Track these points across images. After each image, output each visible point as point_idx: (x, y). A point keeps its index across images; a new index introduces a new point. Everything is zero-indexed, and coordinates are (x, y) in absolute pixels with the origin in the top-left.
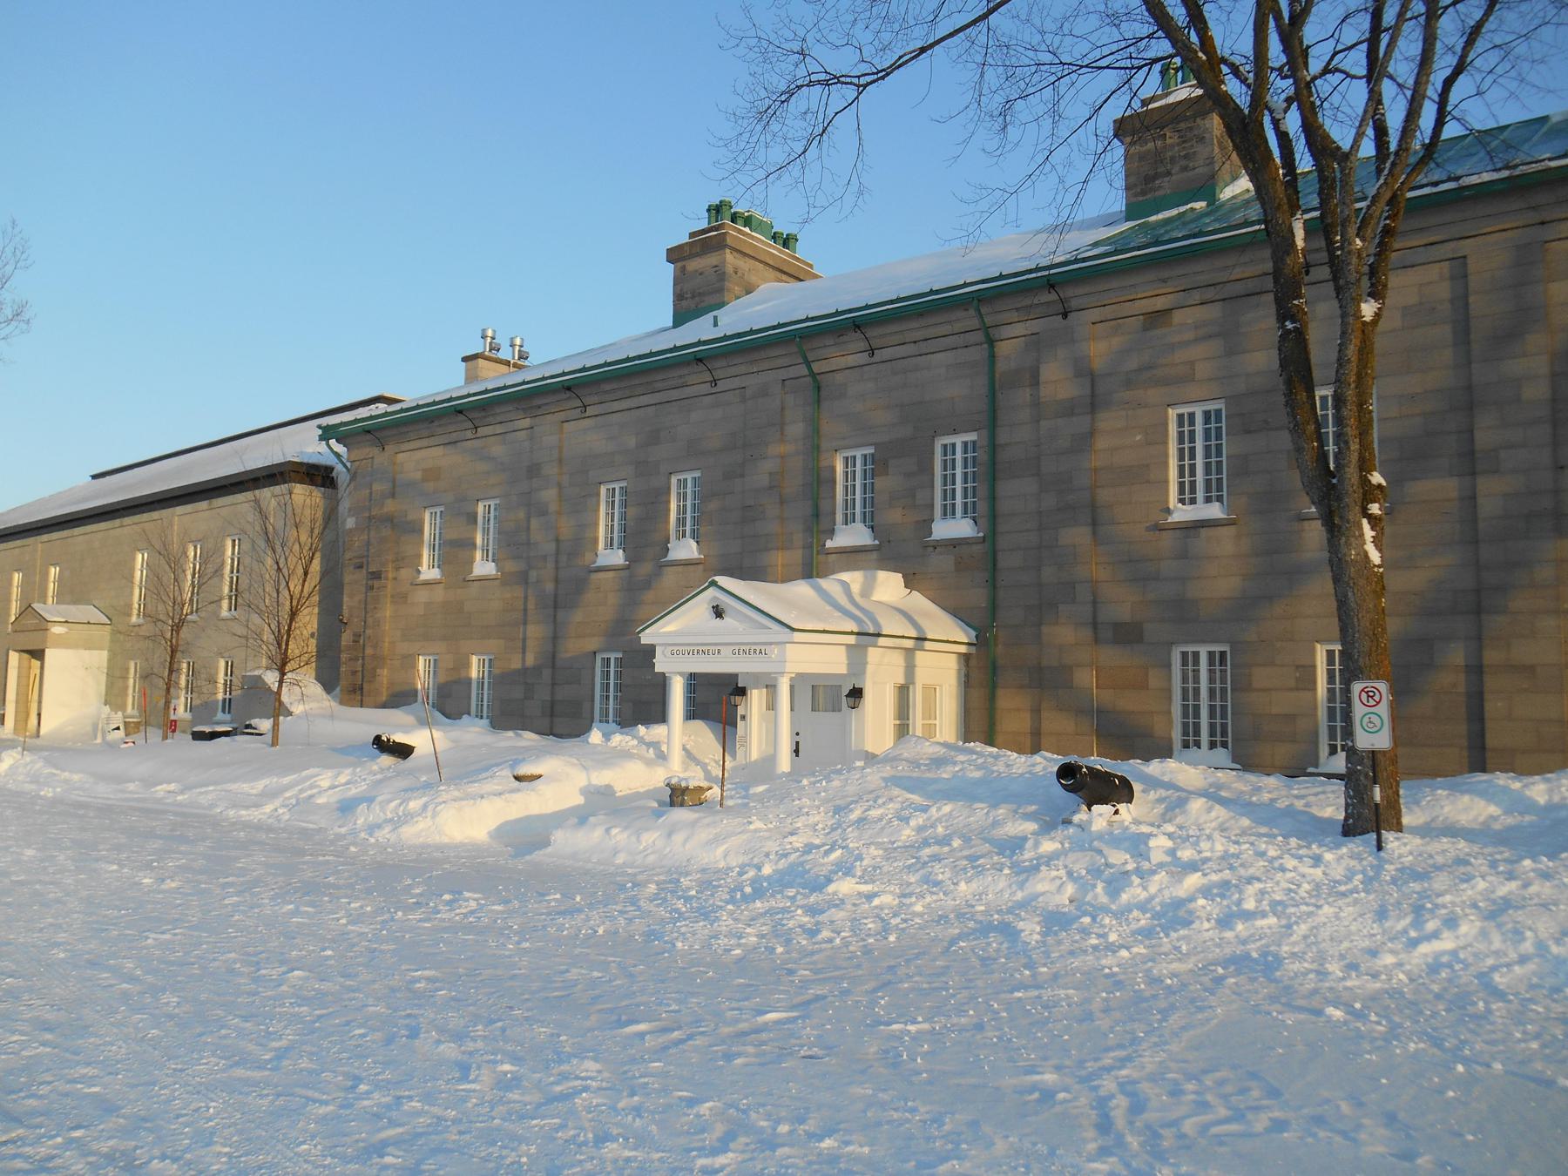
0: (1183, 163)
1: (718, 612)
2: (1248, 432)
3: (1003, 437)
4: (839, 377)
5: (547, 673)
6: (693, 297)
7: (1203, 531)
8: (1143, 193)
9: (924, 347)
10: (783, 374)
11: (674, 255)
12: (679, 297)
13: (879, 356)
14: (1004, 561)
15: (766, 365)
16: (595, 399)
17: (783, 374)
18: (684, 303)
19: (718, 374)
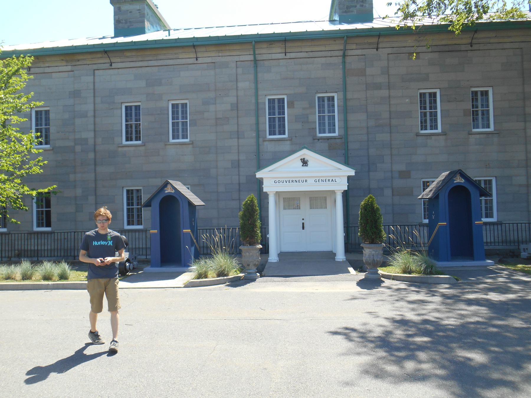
0: (362, 4)
1: (305, 162)
2: (449, 102)
4: (266, 63)
6: (126, 23)
7: (433, 137)
8: (346, 12)
9: (311, 54)
10: (237, 58)
12: (117, 22)
13: (289, 56)
14: (351, 146)
15: (228, 54)
16: (119, 60)
17: (237, 58)
18: (121, 25)
19: (199, 55)
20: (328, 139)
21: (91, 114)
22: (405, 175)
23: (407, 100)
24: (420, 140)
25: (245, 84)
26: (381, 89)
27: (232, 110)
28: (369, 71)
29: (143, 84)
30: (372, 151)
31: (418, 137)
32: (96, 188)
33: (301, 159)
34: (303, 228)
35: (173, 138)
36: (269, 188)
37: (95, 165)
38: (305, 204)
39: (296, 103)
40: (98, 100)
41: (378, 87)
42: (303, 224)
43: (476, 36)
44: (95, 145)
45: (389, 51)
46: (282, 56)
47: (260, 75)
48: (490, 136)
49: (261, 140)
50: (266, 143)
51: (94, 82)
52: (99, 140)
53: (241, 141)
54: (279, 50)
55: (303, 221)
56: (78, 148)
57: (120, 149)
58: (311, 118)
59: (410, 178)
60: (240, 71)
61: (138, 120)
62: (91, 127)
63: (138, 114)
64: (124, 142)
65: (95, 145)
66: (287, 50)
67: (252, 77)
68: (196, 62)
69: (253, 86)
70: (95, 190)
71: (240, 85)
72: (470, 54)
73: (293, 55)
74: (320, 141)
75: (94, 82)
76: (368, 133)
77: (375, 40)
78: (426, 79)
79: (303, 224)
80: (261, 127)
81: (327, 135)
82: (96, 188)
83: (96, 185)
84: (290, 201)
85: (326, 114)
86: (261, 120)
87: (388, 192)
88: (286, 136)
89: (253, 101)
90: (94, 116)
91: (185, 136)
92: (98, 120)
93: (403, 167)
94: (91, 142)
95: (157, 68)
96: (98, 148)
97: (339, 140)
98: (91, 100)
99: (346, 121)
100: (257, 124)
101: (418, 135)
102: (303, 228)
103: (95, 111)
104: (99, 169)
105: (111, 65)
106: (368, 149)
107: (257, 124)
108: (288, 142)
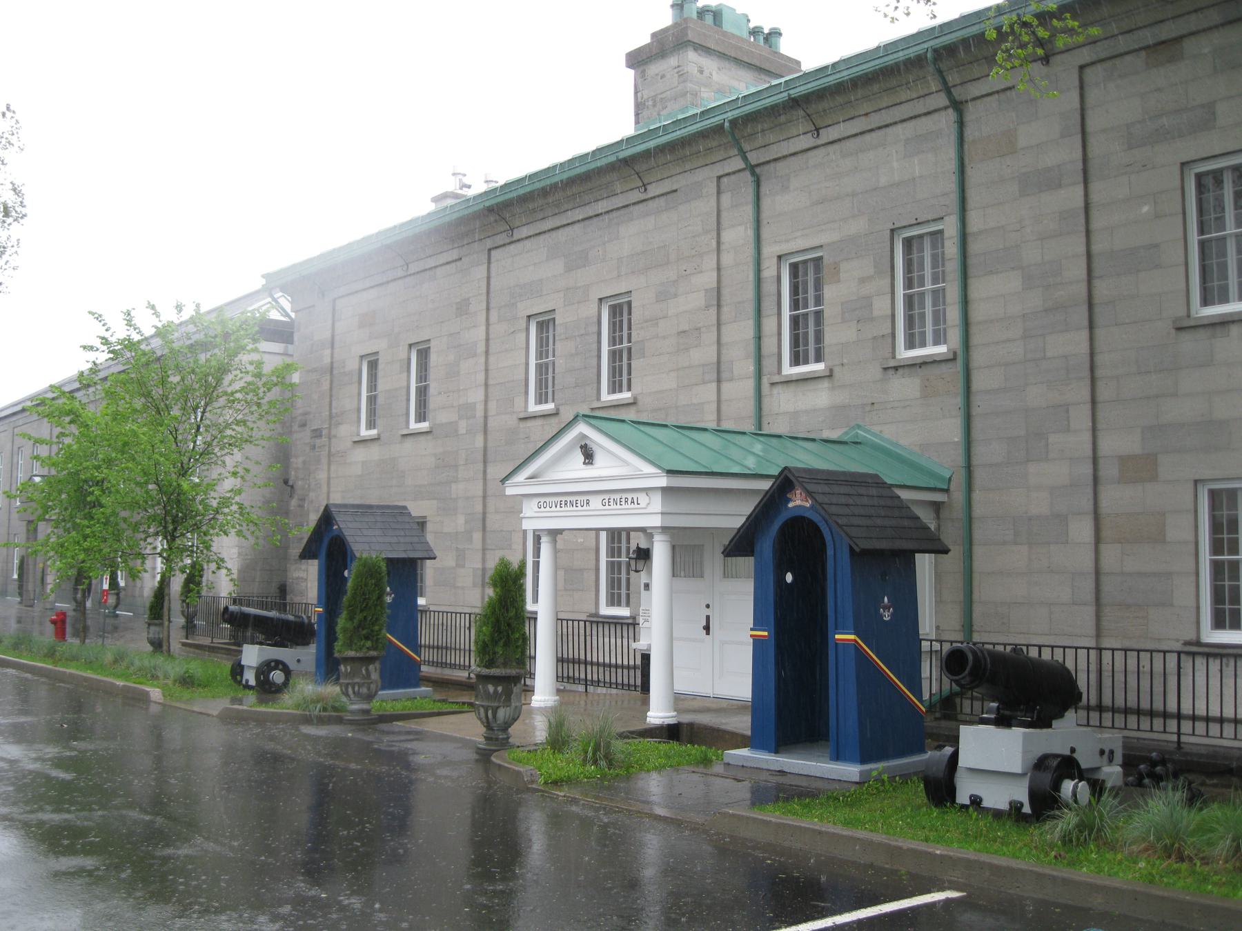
1: (589, 456)
3: (975, 222)
5: (477, 536)
11: (638, 60)
14: (978, 383)
21: (481, 348)
22: (1140, 468)
23: (1145, 209)
24: (1189, 344)
25: (738, 235)
26: (1060, 186)
27: (707, 307)
29: (558, 266)
32: (484, 513)
33: (581, 447)
37: (485, 462)
39: (844, 266)
40: (494, 316)
42: (708, 618)
44: (486, 417)
45: (1085, 55)
46: (806, 141)
47: (766, 203)
49: (765, 381)
50: (776, 390)
51: (489, 278)
52: (492, 405)
55: (708, 612)
56: (463, 426)
57: (523, 425)
58: (881, 306)
59: (1154, 478)
60: (726, 199)
62: (481, 377)
65: (486, 417)
66: (819, 123)
67: (749, 210)
68: (643, 196)
69: (751, 233)
70: (484, 520)
71: (727, 236)
74: (901, 371)
75: (489, 278)
78: (1206, 119)
79: (708, 618)
80: (769, 345)
82: (484, 513)
83: (485, 506)
86: (769, 325)
87: (1082, 530)
89: (751, 276)
90: (487, 352)
92: (492, 359)
94: (480, 413)
96: (492, 423)
97: (950, 365)
98: (482, 318)
99: (965, 302)
100: (759, 338)
103: (487, 340)
107: (759, 338)
108: (825, 384)
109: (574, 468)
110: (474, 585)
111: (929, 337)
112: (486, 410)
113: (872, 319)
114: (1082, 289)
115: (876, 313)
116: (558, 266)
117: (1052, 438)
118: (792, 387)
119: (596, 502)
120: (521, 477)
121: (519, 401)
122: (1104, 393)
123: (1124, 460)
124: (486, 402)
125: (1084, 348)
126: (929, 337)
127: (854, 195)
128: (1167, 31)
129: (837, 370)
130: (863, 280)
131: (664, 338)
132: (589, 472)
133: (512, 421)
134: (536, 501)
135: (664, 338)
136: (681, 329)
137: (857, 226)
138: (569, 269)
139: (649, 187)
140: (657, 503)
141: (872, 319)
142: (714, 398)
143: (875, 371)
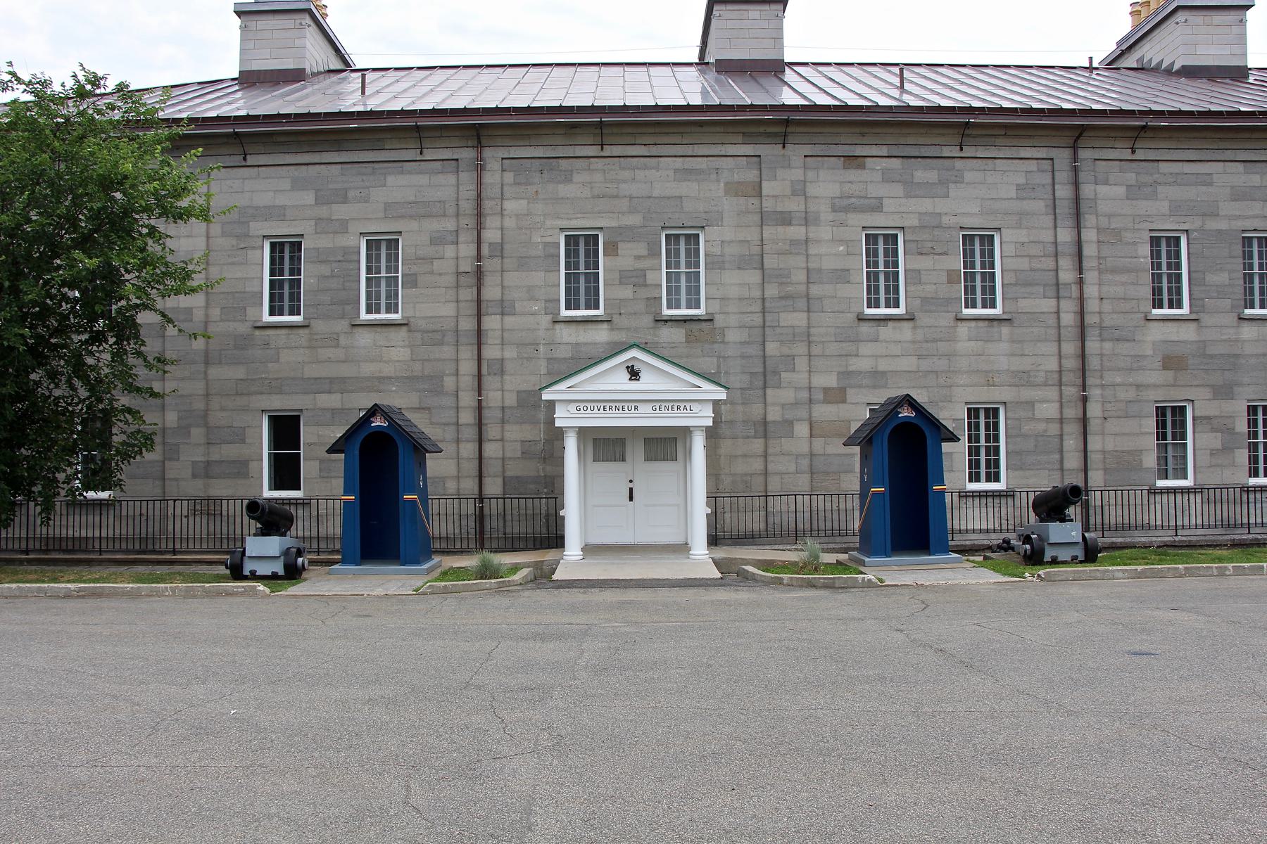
1: (634, 374)
5: (197, 433)
7: (890, 324)
13: (608, 151)
20: (685, 321)
24: (865, 328)
26: (790, 224)
28: (767, 188)
29: (309, 198)
30: (772, 348)
31: (862, 324)
34: (631, 499)
35: (369, 311)
36: (564, 417)
38: (636, 451)
39: (621, 245)
41: (785, 219)
42: (631, 489)
43: (967, 132)
48: (995, 323)
50: (558, 326)
53: (508, 319)
54: (590, 140)
55: (631, 485)
57: (257, 332)
58: (651, 277)
59: (844, 401)
61: (295, 271)
63: (295, 259)
64: (267, 318)
72: (959, 164)
73: (617, 150)
76: (764, 311)
77: (780, 129)
79: (631, 489)
81: (684, 312)
84: (606, 445)
85: (683, 269)
87: (802, 430)
88: (600, 312)
91: (392, 308)
93: (831, 381)
95: (339, 166)
96: (212, 329)
101: (862, 319)
102: (631, 499)
104: (214, 372)
105: (245, 159)
106: (764, 343)
108: (605, 326)
109: (619, 382)
110: (194, 476)
111: (683, 302)
112: (207, 315)
113: (646, 286)
114: (803, 288)
115: (649, 282)
116: (309, 198)
117: (783, 375)
118: (573, 326)
119: (643, 408)
120: (562, 386)
121: (251, 312)
122: (816, 350)
123: (826, 390)
124: (207, 306)
125: (804, 323)
126: (683, 302)
127: (631, 197)
128: (859, 151)
129: (616, 318)
130: (638, 258)
131: (440, 274)
132: (634, 385)
133: (243, 328)
134: (574, 406)
135: (440, 274)
136: (461, 269)
137: (634, 220)
138: (319, 201)
139: (425, 151)
140: (708, 412)
141: (646, 286)
142: (499, 327)
143: (647, 320)
